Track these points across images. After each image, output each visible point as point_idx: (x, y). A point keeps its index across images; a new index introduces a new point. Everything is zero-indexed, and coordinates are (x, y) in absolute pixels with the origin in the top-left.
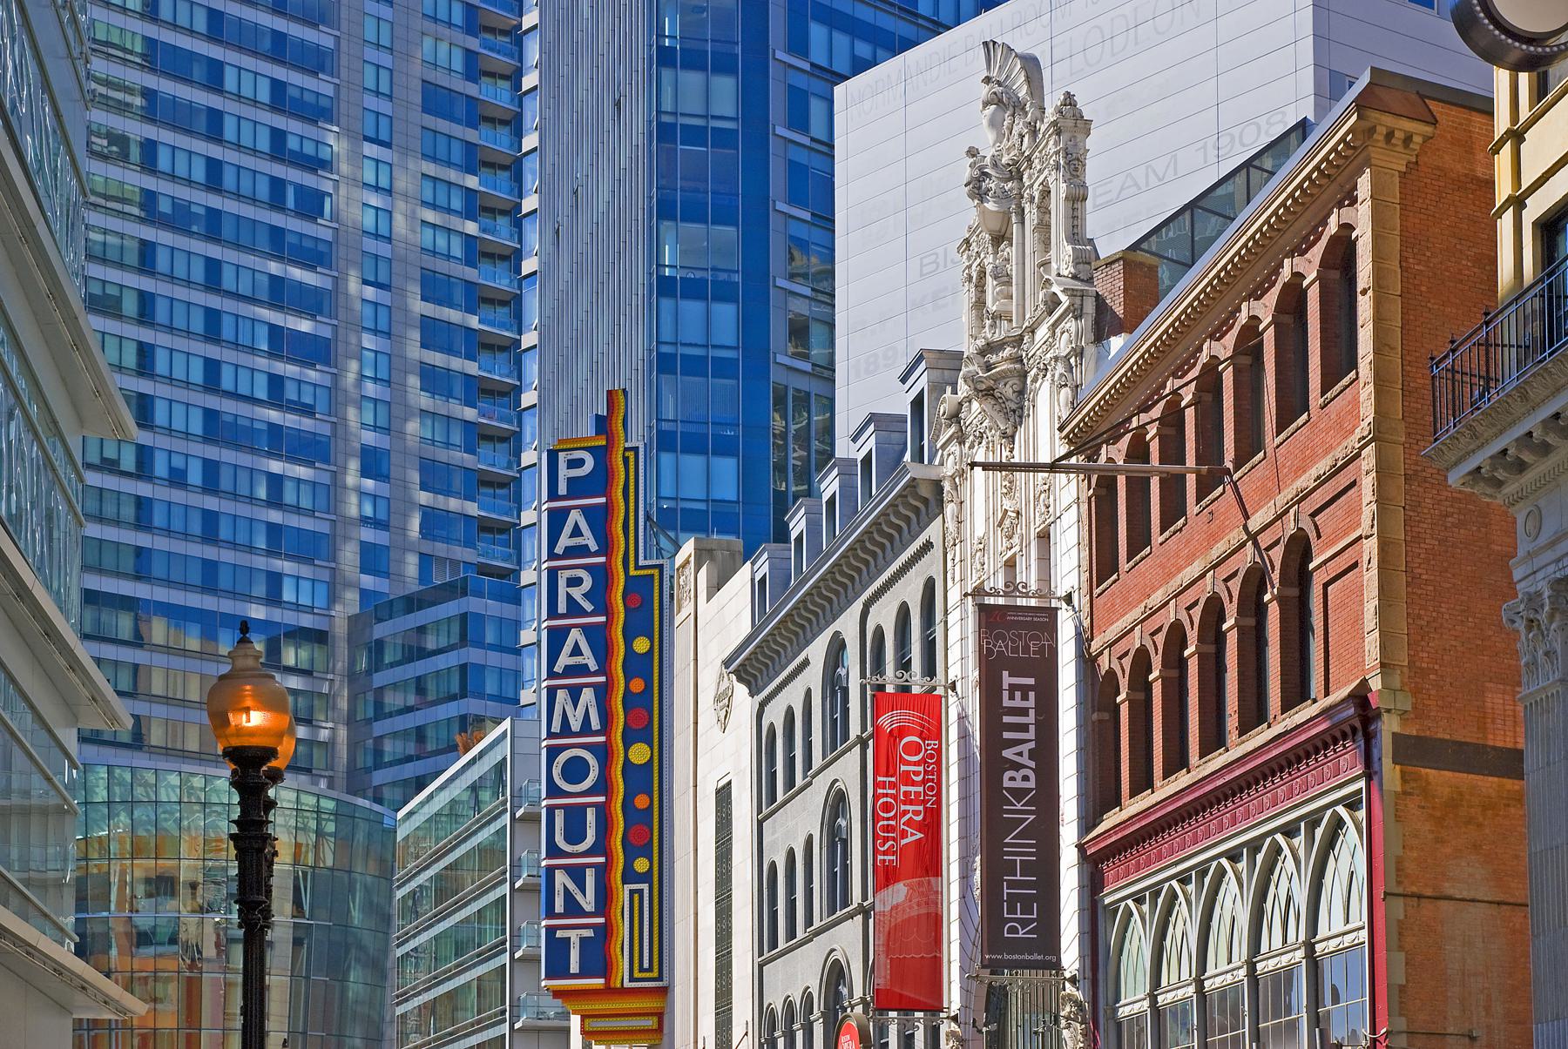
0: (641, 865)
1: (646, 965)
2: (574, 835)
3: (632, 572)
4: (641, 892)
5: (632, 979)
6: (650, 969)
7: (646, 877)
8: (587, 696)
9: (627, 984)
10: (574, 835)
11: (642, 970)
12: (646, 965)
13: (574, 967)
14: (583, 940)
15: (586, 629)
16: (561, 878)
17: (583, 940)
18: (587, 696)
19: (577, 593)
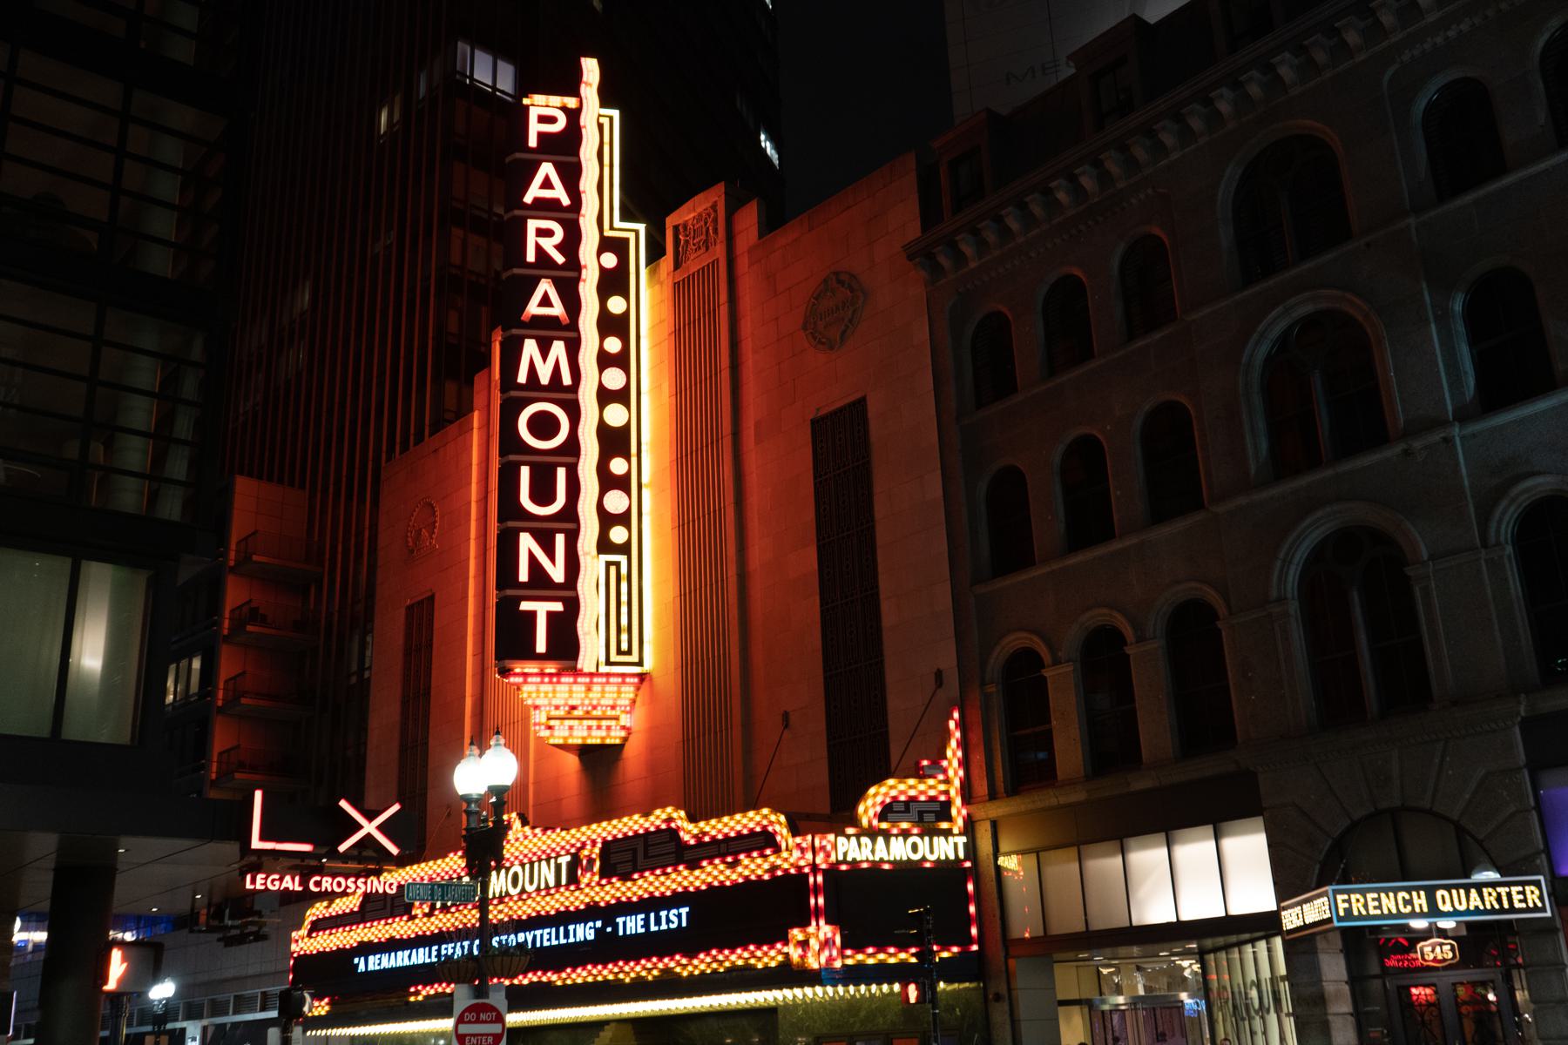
0: (618, 535)
1: (624, 647)
2: (543, 494)
3: (608, 233)
4: (618, 564)
5: (608, 663)
6: (629, 652)
7: (625, 549)
8: (558, 349)
9: (604, 669)
10: (543, 494)
11: (619, 652)
12: (624, 647)
13: (541, 647)
14: (550, 615)
15: (557, 283)
16: (527, 542)
17: (550, 615)
18: (558, 349)
19: (548, 245)
